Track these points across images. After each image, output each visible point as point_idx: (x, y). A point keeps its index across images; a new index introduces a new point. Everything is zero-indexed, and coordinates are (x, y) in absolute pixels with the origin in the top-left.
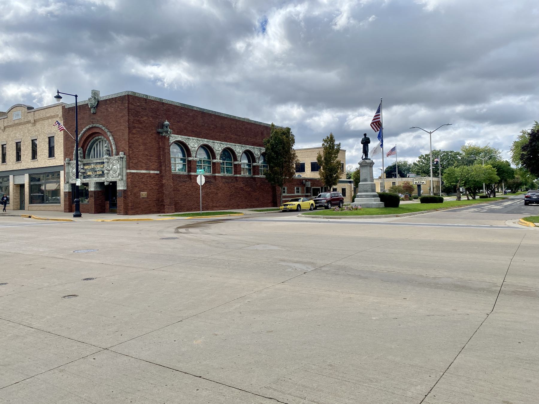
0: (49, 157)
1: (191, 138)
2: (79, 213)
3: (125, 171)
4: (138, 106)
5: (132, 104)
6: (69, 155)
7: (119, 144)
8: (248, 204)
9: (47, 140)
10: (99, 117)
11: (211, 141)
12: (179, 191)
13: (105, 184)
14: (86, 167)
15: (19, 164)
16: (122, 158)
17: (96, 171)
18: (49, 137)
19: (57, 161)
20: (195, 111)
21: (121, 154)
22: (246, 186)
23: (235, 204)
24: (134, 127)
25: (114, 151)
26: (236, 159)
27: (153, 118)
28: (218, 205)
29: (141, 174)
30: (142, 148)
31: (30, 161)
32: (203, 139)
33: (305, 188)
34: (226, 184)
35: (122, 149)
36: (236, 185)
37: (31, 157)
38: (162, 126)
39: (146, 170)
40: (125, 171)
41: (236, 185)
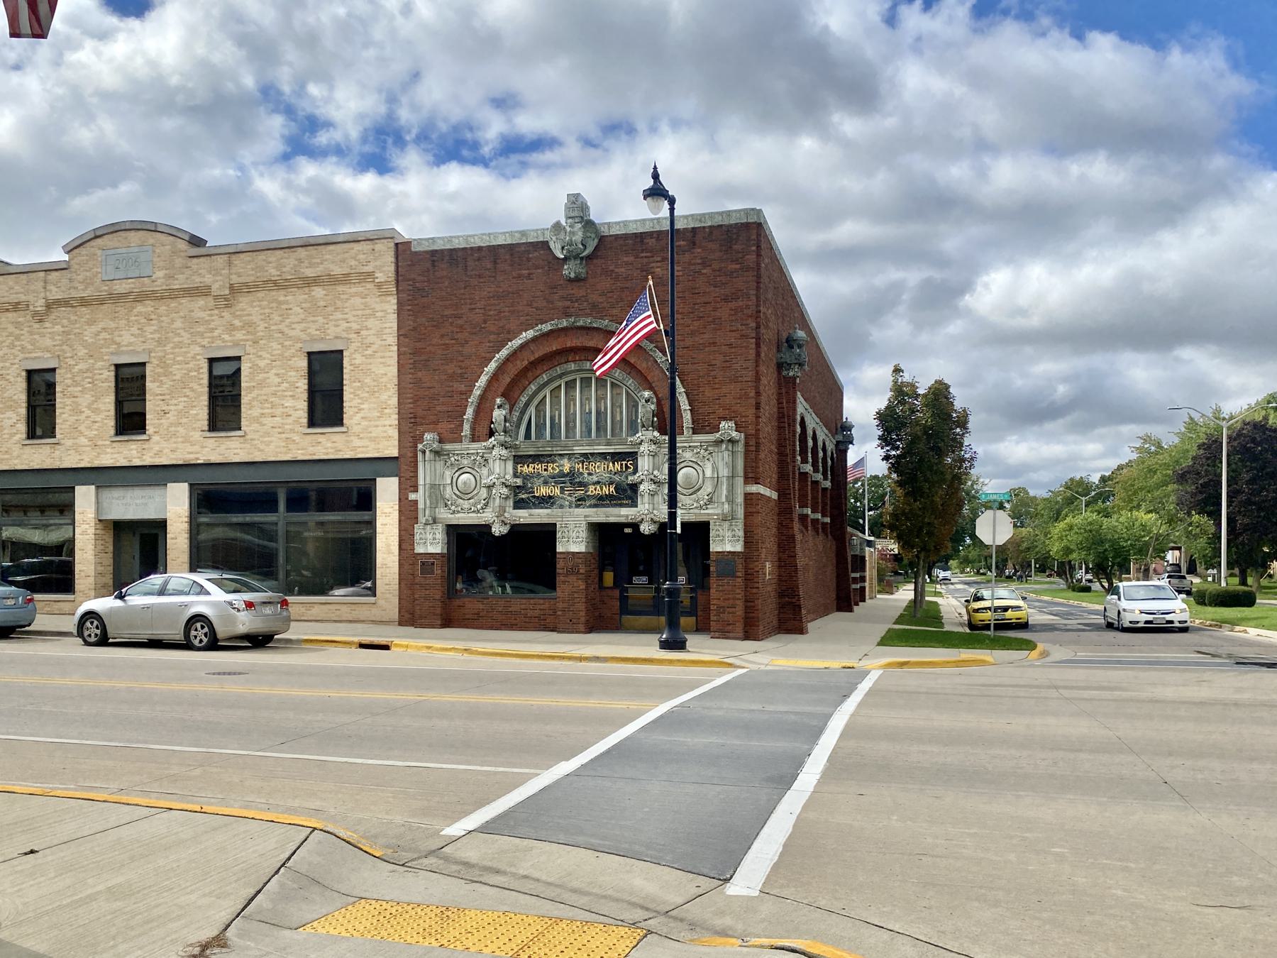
0: (312, 423)
3: (740, 489)
6: (436, 423)
7: (709, 393)
9: (304, 363)
10: (603, 294)
13: (642, 528)
14: (526, 469)
15: (133, 446)
16: (732, 441)
17: (581, 484)
18: (309, 354)
19: (357, 442)
21: (727, 427)
25: (687, 417)
31: (197, 435)
35: (721, 412)
37: (205, 424)
40: (740, 489)
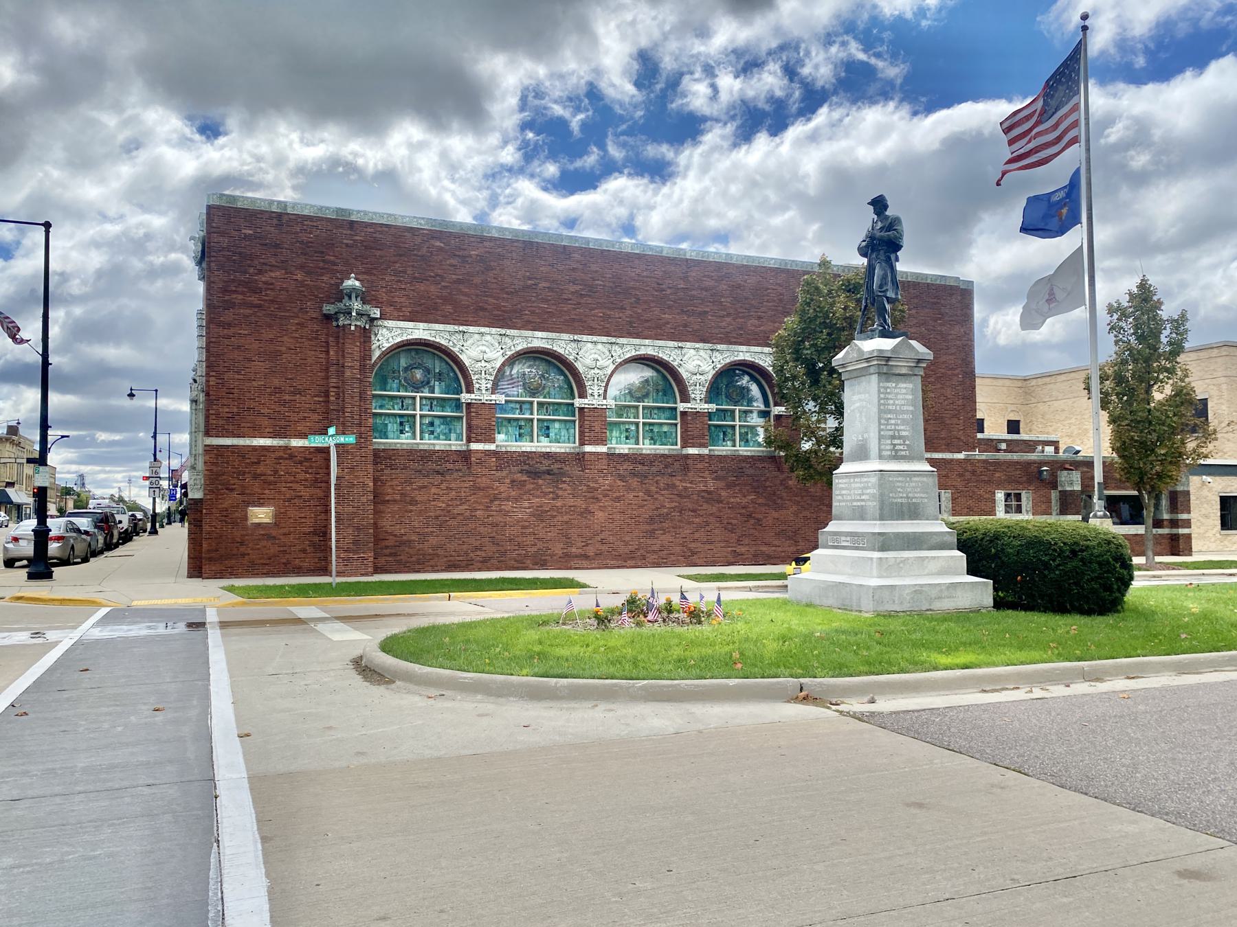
1: (471, 329)
2: (41, 568)
4: (246, 237)
5: (222, 234)
8: (743, 549)
11: (565, 336)
12: (413, 502)
20: (492, 239)
22: (729, 486)
23: (678, 549)
24: (229, 305)
26: (685, 398)
27: (308, 273)
28: (591, 551)
29: (255, 448)
30: (259, 366)
32: (529, 333)
33: (1054, 495)
34: (634, 482)
36: (680, 485)
38: (341, 295)
39: (274, 435)
41: (680, 485)
